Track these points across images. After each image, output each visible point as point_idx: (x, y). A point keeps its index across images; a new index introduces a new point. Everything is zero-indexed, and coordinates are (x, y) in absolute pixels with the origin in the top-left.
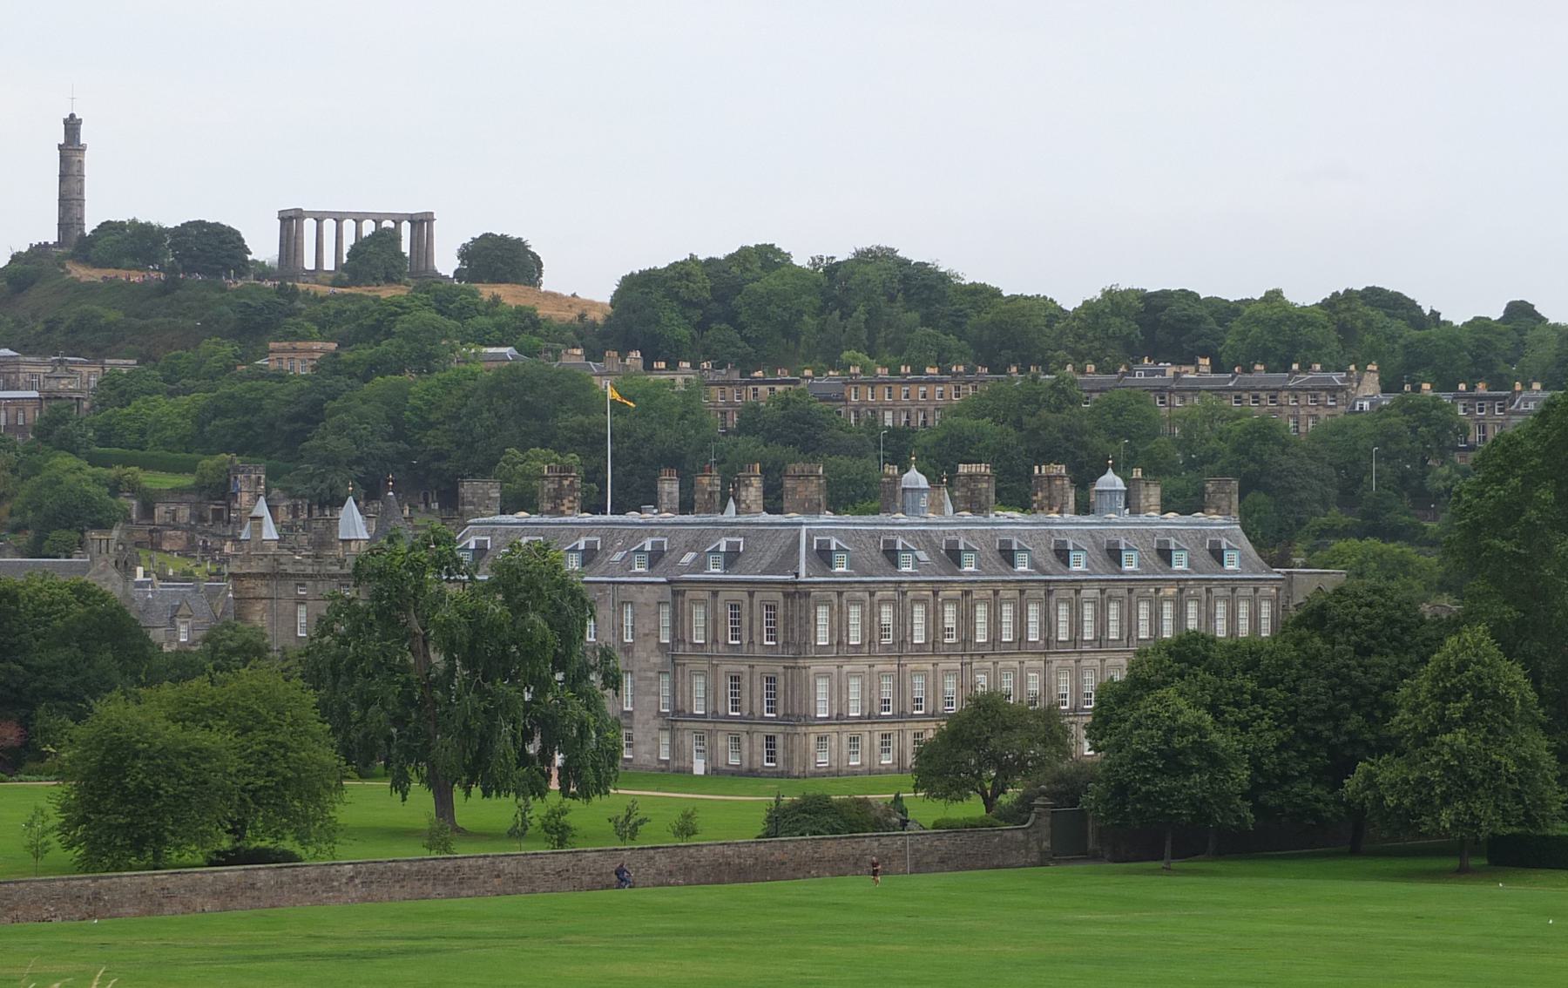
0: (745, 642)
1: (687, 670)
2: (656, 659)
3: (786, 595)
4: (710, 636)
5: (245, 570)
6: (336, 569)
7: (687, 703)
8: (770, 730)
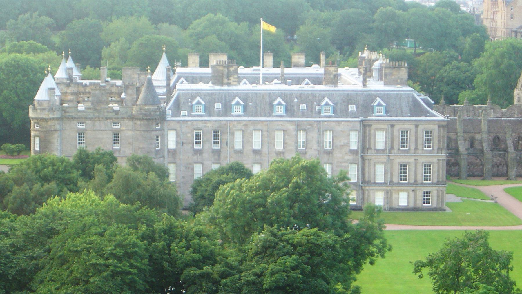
0: (413, 147)
1: (372, 162)
2: (350, 157)
3: (439, 127)
4: (389, 146)
7: (372, 177)
8: (428, 189)
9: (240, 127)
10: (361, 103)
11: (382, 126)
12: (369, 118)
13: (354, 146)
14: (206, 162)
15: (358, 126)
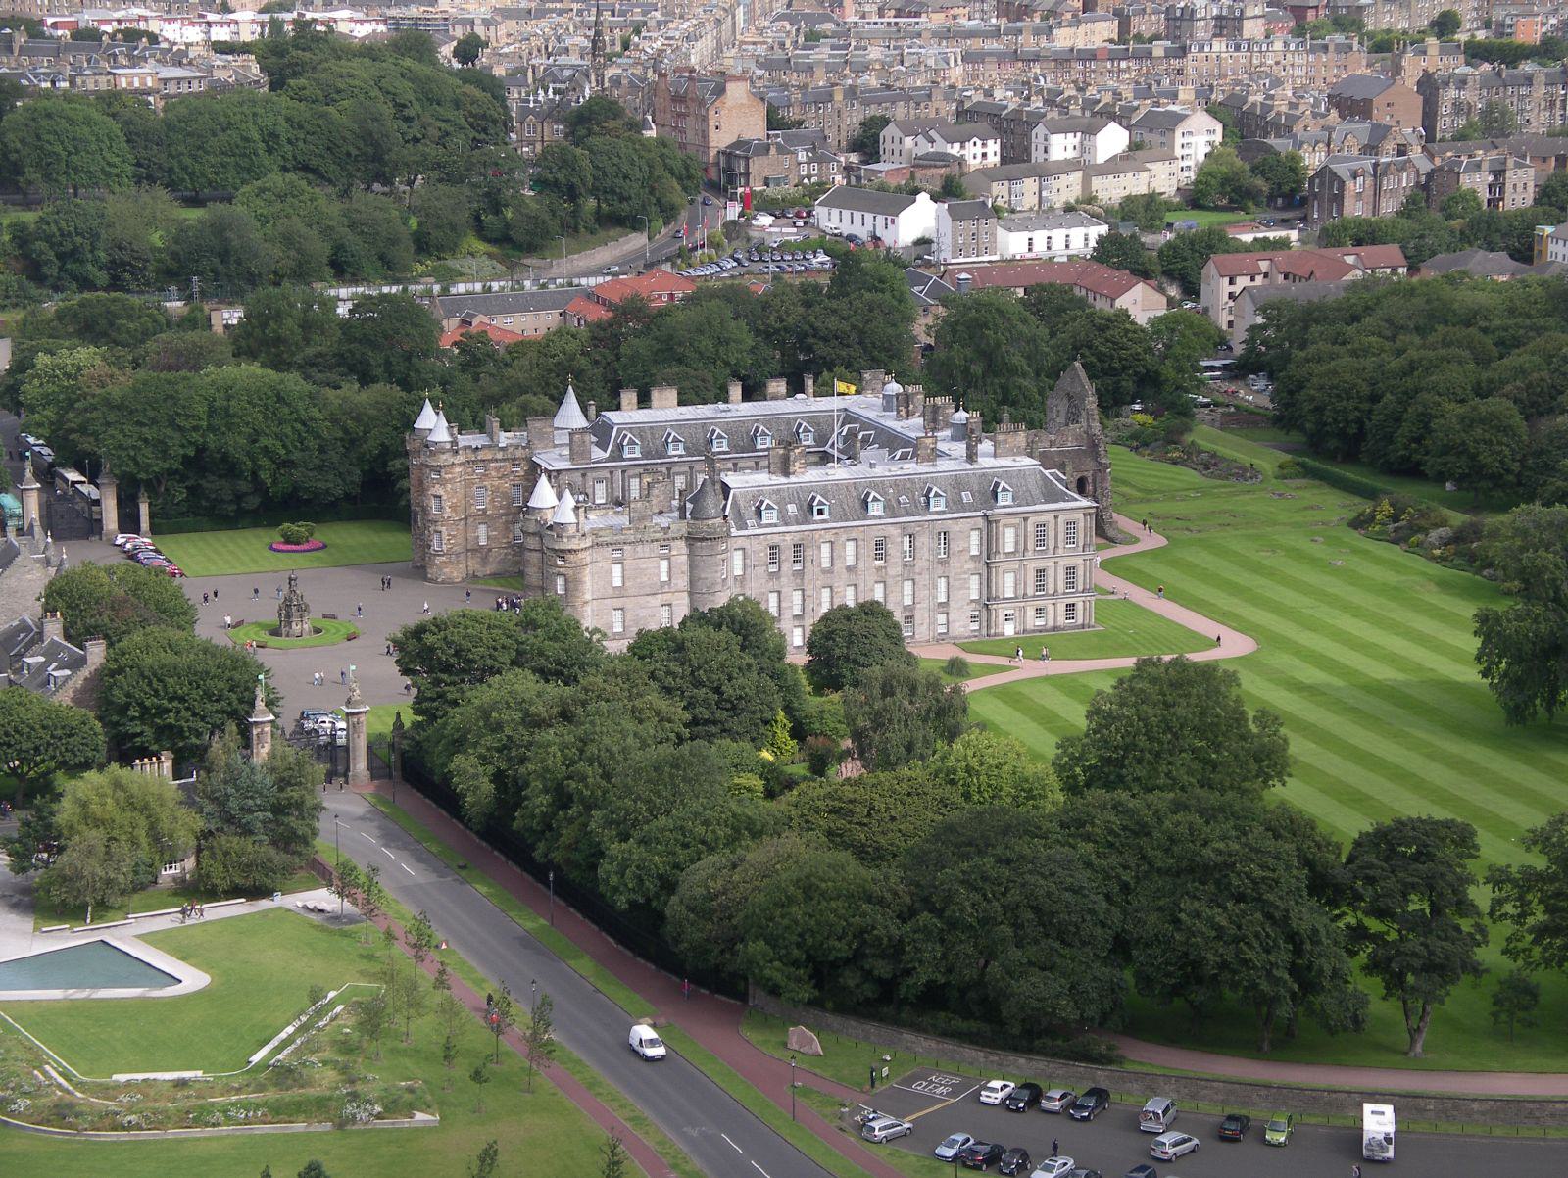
1: (1000, 570)
2: (971, 566)
5: (583, 546)
6: (658, 536)
8: (1071, 601)
9: (829, 536)
10: (976, 487)
11: (1013, 521)
12: (997, 511)
13: (975, 551)
14: (784, 590)
15: (981, 523)
